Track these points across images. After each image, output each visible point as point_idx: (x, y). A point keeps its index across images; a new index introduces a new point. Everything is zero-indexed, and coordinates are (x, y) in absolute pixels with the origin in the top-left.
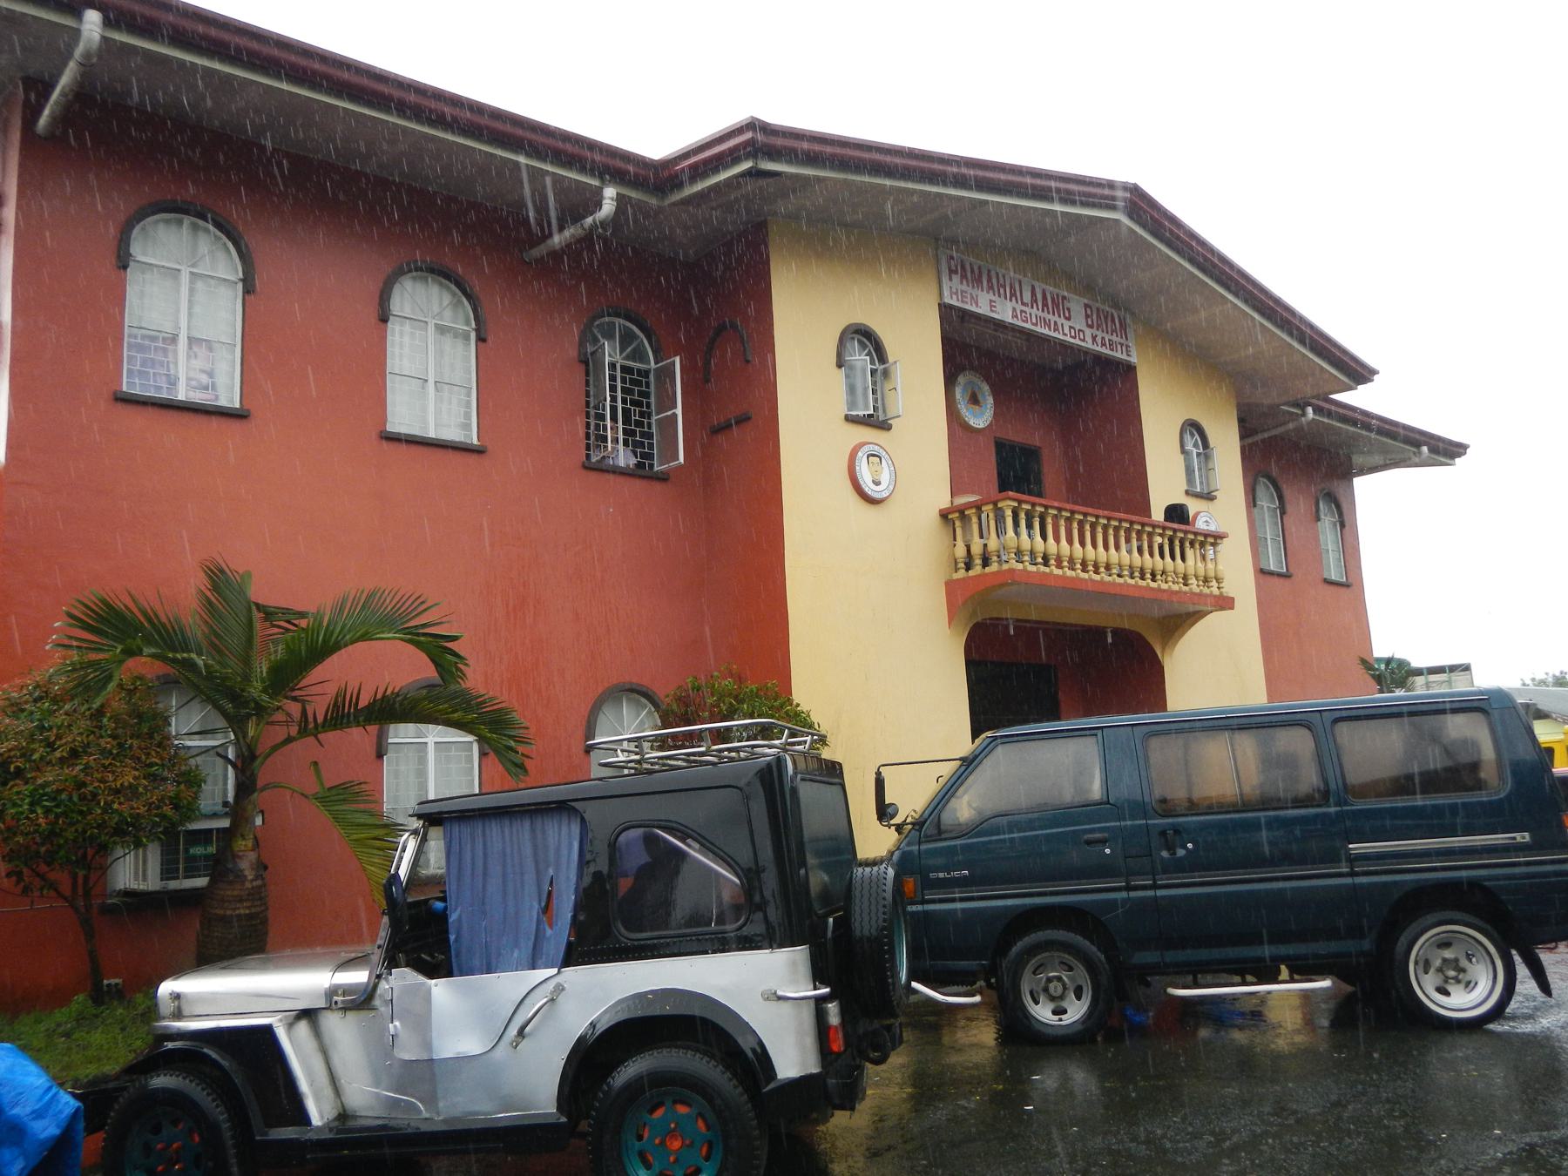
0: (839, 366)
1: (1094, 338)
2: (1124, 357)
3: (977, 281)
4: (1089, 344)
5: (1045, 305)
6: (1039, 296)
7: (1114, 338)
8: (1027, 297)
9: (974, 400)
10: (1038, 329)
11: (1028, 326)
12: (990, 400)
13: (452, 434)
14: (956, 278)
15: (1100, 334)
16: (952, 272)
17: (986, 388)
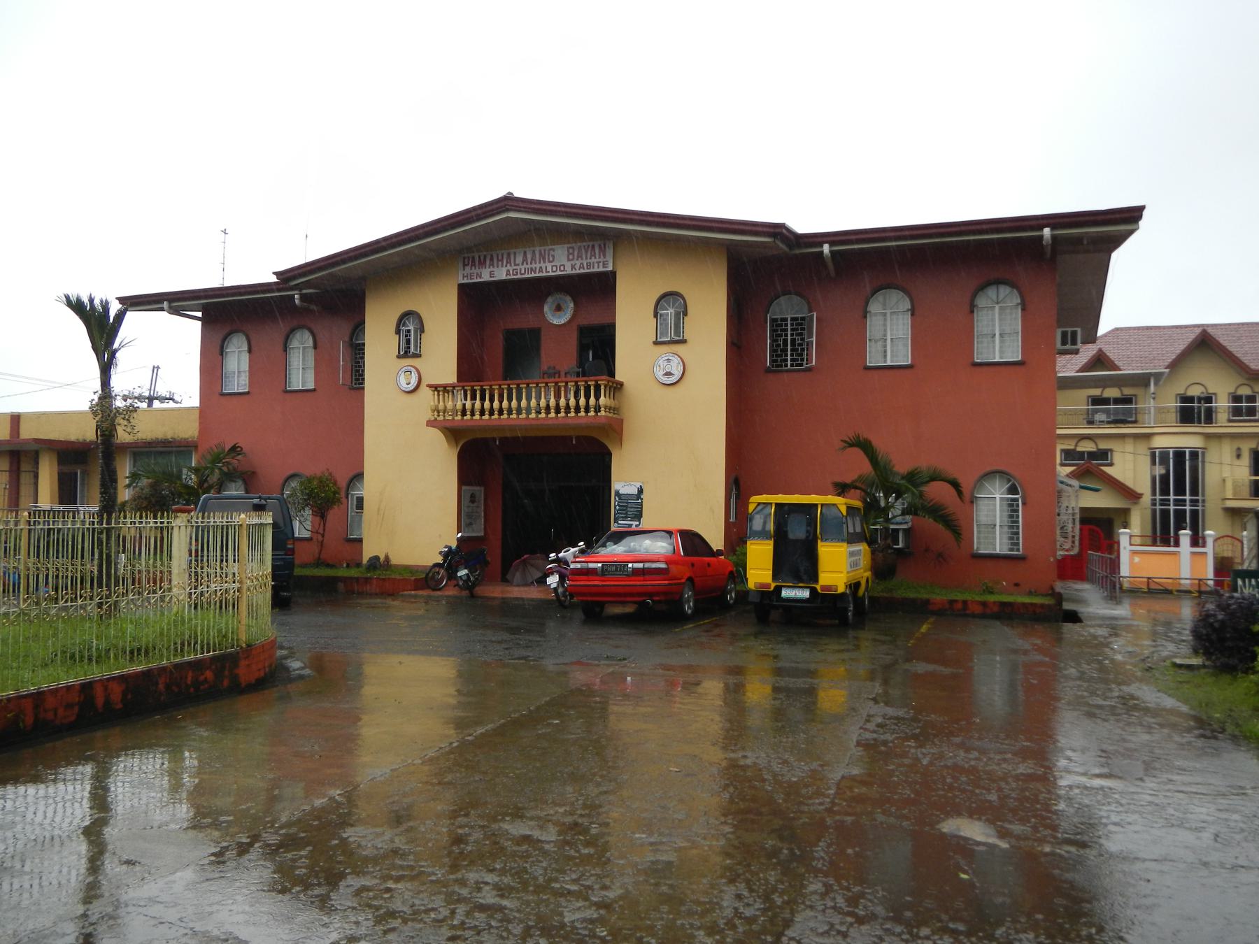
0: (398, 332)
1: (573, 267)
2: (601, 269)
3: (482, 263)
4: (569, 271)
5: (533, 259)
6: (529, 256)
7: (593, 259)
8: (519, 259)
9: (559, 308)
10: (526, 276)
11: (519, 276)
12: (572, 305)
13: (311, 385)
14: (468, 268)
15: (578, 263)
16: (464, 265)
17: (568, 298)
